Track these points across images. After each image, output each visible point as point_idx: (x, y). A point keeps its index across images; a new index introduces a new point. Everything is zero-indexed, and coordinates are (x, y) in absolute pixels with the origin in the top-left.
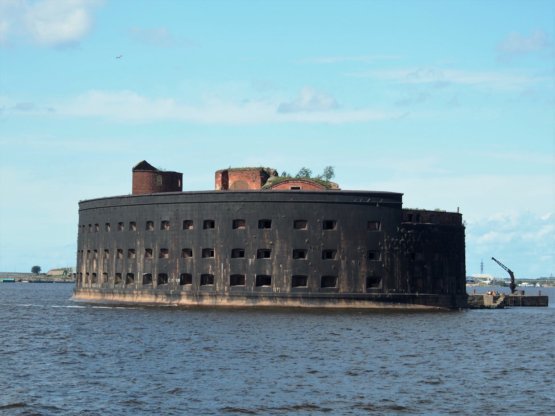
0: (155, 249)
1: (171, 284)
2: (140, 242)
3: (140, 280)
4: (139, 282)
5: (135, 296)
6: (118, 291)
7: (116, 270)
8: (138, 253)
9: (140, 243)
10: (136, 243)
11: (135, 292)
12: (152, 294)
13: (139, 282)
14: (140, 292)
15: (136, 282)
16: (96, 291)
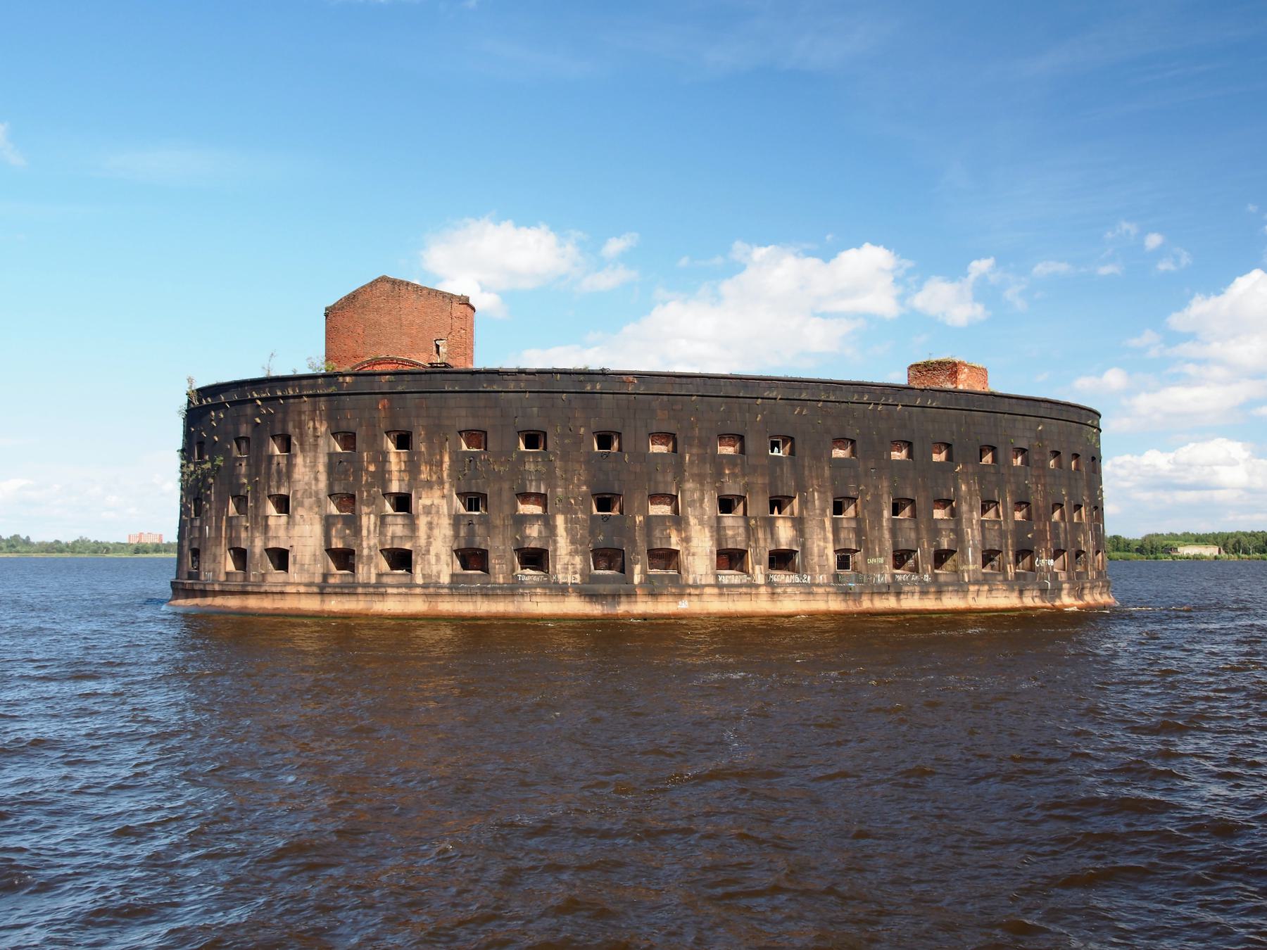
0: (1005, 501)
1: (1041, 569)
2: (968, 484)
3: (975, 563)
4: (971, 567)
5: (970, 596)
6: (917, 589)
7: (895, 544)
8: (965, 508)
9: (969, 490)
10: (957, 489)
11: (972, 588)
12: (1012, 590)
13: (971, 567)
14: (986, 588)
15: (965, 567)
16: (821, 590)
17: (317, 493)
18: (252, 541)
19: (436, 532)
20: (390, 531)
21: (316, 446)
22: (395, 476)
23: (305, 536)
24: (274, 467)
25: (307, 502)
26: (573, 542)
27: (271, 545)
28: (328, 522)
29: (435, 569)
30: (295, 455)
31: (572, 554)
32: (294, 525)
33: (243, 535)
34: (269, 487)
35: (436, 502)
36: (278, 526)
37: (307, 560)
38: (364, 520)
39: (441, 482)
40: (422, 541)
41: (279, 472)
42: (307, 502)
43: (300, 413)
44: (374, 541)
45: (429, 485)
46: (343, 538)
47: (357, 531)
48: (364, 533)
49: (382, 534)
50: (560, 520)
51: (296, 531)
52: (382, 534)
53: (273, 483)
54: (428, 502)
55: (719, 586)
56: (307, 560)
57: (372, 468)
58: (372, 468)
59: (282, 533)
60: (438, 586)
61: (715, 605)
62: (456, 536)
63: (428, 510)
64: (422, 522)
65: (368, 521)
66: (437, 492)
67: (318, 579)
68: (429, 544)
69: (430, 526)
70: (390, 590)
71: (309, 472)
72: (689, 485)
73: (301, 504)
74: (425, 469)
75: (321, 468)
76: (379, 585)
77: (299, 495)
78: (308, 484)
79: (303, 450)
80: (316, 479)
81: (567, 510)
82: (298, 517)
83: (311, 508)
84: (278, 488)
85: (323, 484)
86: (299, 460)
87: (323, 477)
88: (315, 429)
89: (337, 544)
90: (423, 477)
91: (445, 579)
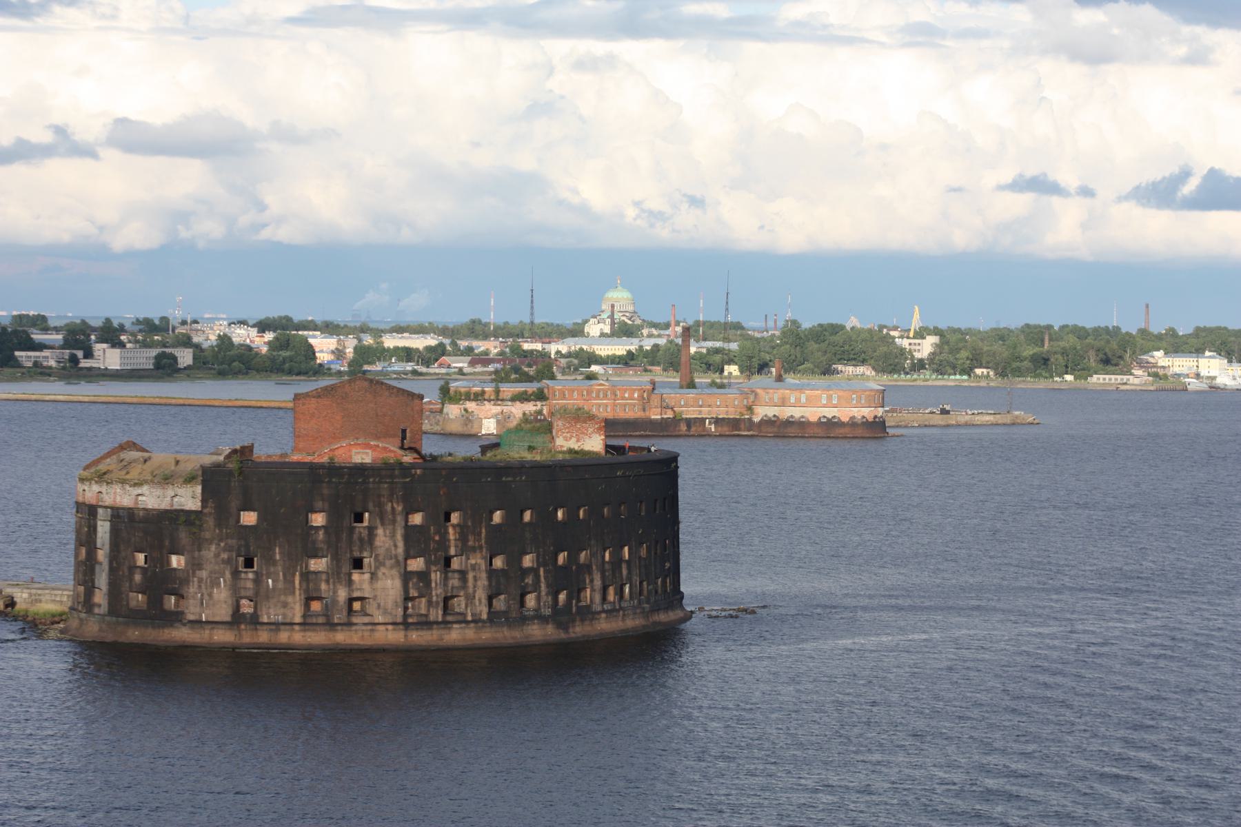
17: (396, 556)
18: (335, 592)
19: (479, 583)
20: (451, 583)
21: (394, 522)
22: (452, 543)
23: (389, 587)
24: (355, 536)
25: (388, 563)
26: (548, 586)
27: (356, 594)
28: (406, 577)
29: (478, 609)
30: (376, 528)
31: (547, 595)
32: (377, 579)
33: (323, 586)
34: (351, 551)
35: (479, 561)
36: (361, 582)
37: (390, 605)
38: (433, 575)
39: (481, 547)
40: (471, 590)
41: (361, 540)
42: (388, 563)
43: (379, 496)
44: (439, 591)
45: (473, 549)
46: (418, 589)
47: (428, 583)
48: (433, 585)
49: (445, 585)
50: (542, 570)
51: (379, 584)
52: (445, 585)
53: (355, 548)
54: (473, 562)
55: (604, 611)
56: (390, 605)
57: (437, 538)
58: (437, 538)
59: (366, 586)
60: (483, 621)
61: (604, 625)
62: (490, 585)
63: (474, 567)
64: (470, 576)
65: (436, 576)
66: (479, 555)
67: (399, 620)
68: (475, 592)
69: (475, 579)
70: (455, 626)
71: (388, 540)
72: (593, 542)
73: (383, 565)
74: (471, 538)
75: (399, 537)
76: (445, 622)
77: (381, 558)
78: (388, 550)
79: (383, 524)
80: (396, 546)
81: (545, 565)
82: (380, 574)
83: (392, 568)
84: (361, 552)
85: (401, 550)
86: (380, 531)
87: (401, 544)
88: (393, 508)
89: (413, 593)
90: (470, 543)
91: (485, 616)
